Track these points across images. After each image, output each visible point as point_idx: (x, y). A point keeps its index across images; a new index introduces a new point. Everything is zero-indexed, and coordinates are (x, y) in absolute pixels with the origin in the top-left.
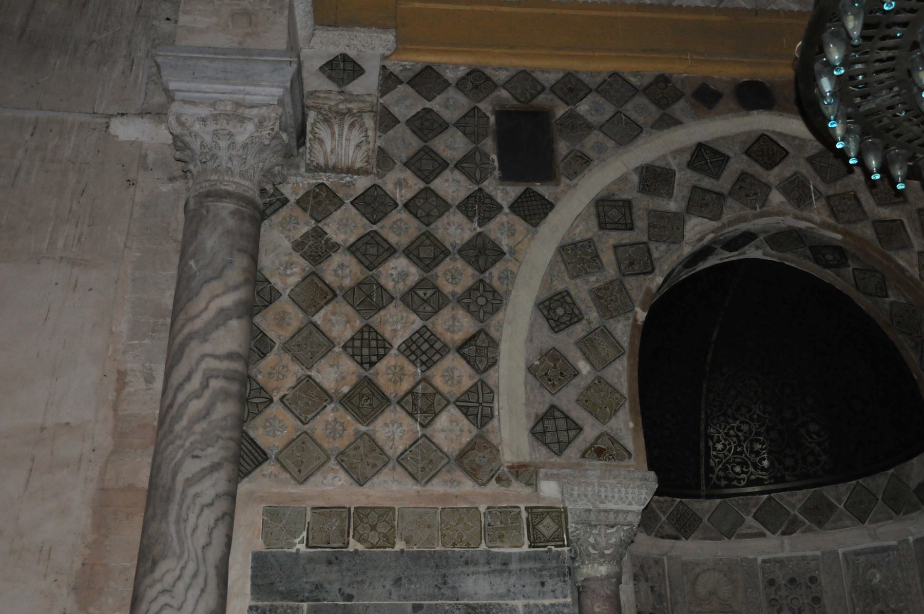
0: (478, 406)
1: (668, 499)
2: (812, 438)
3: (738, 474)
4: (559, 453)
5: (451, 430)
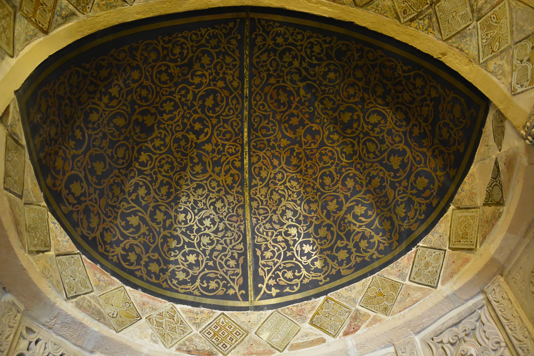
1: (206, 310)
2: (361, 221)
3: (290, 280)
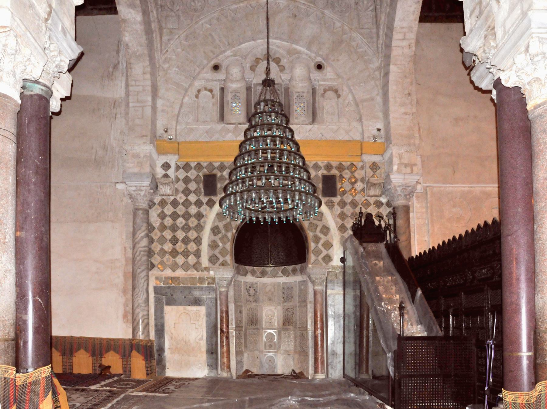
0: (197, 254)
4: (214, 265)
5: (192, 259)
